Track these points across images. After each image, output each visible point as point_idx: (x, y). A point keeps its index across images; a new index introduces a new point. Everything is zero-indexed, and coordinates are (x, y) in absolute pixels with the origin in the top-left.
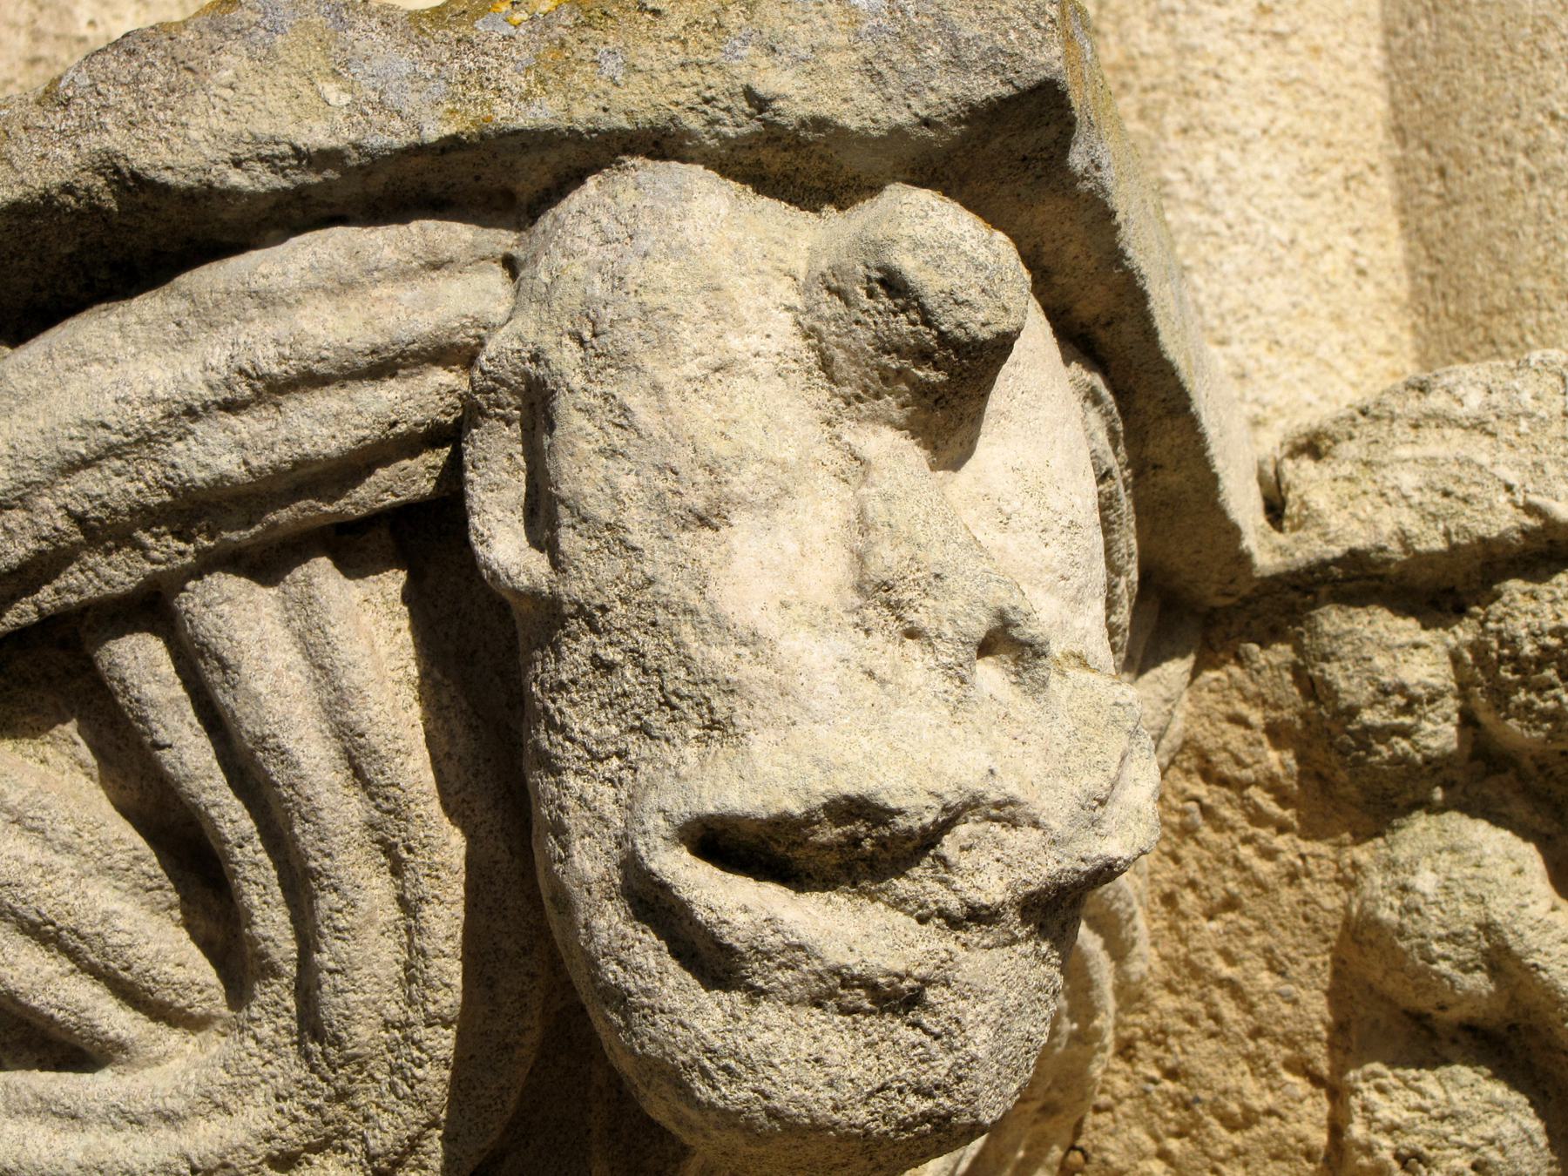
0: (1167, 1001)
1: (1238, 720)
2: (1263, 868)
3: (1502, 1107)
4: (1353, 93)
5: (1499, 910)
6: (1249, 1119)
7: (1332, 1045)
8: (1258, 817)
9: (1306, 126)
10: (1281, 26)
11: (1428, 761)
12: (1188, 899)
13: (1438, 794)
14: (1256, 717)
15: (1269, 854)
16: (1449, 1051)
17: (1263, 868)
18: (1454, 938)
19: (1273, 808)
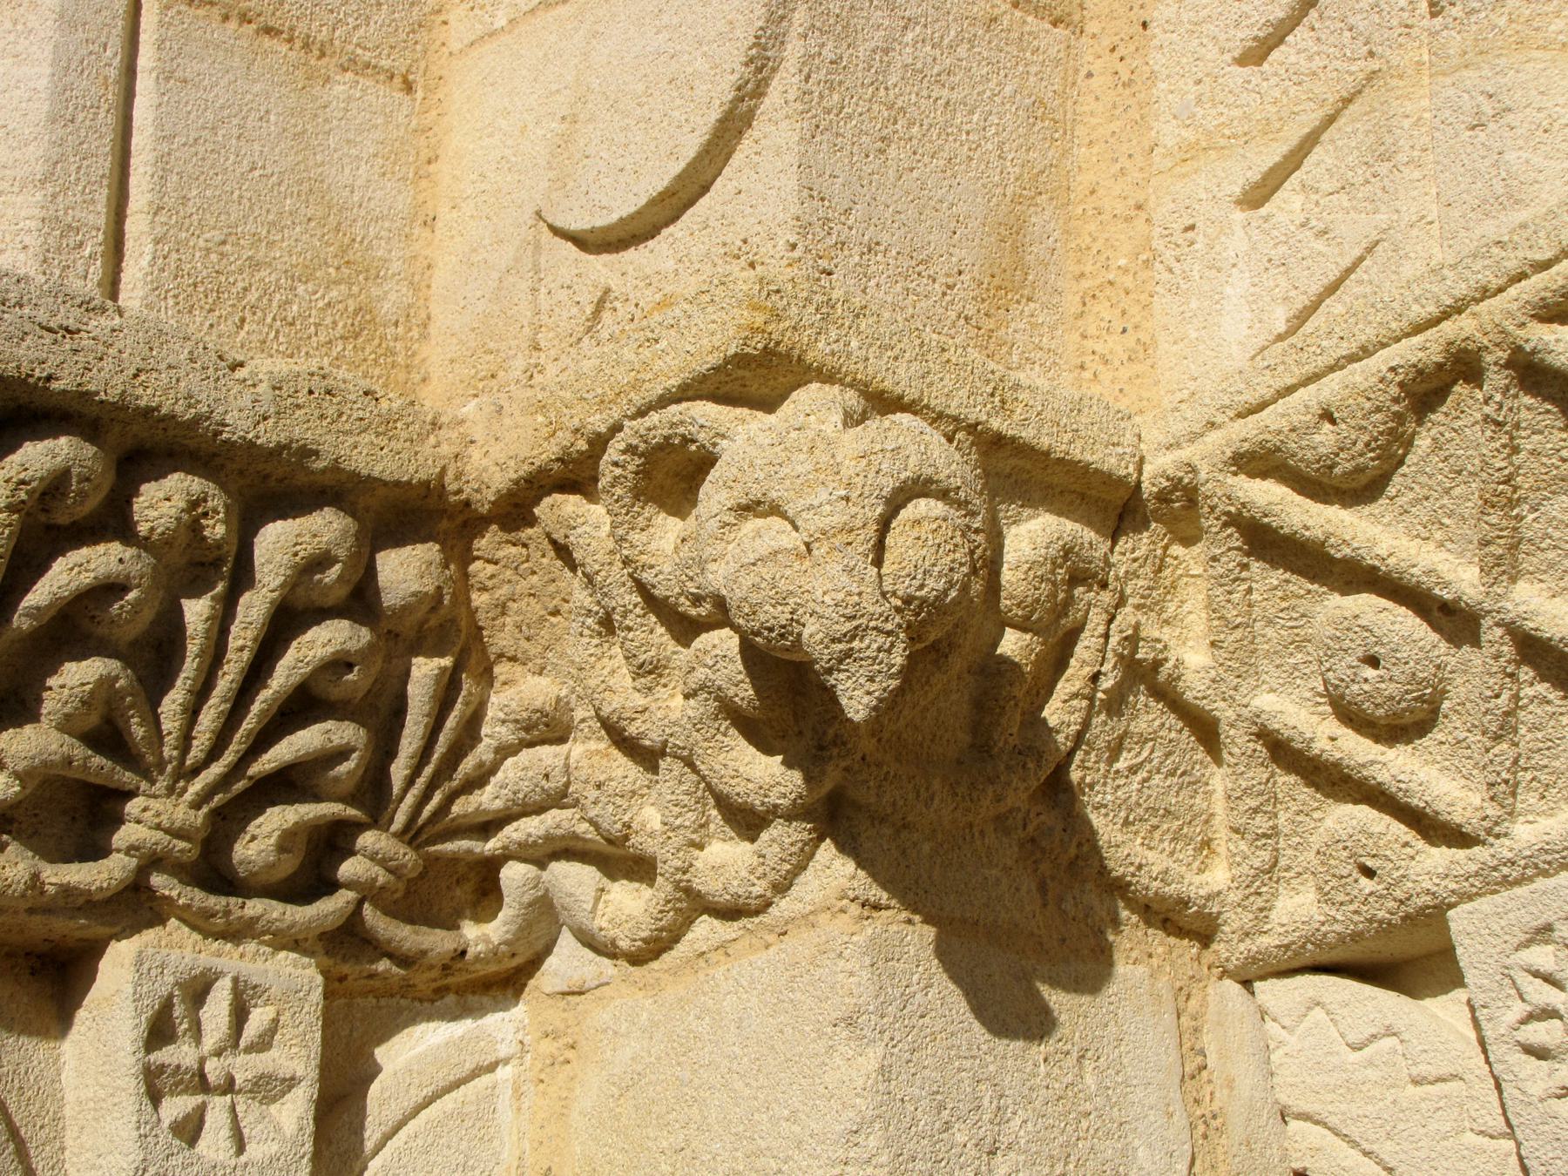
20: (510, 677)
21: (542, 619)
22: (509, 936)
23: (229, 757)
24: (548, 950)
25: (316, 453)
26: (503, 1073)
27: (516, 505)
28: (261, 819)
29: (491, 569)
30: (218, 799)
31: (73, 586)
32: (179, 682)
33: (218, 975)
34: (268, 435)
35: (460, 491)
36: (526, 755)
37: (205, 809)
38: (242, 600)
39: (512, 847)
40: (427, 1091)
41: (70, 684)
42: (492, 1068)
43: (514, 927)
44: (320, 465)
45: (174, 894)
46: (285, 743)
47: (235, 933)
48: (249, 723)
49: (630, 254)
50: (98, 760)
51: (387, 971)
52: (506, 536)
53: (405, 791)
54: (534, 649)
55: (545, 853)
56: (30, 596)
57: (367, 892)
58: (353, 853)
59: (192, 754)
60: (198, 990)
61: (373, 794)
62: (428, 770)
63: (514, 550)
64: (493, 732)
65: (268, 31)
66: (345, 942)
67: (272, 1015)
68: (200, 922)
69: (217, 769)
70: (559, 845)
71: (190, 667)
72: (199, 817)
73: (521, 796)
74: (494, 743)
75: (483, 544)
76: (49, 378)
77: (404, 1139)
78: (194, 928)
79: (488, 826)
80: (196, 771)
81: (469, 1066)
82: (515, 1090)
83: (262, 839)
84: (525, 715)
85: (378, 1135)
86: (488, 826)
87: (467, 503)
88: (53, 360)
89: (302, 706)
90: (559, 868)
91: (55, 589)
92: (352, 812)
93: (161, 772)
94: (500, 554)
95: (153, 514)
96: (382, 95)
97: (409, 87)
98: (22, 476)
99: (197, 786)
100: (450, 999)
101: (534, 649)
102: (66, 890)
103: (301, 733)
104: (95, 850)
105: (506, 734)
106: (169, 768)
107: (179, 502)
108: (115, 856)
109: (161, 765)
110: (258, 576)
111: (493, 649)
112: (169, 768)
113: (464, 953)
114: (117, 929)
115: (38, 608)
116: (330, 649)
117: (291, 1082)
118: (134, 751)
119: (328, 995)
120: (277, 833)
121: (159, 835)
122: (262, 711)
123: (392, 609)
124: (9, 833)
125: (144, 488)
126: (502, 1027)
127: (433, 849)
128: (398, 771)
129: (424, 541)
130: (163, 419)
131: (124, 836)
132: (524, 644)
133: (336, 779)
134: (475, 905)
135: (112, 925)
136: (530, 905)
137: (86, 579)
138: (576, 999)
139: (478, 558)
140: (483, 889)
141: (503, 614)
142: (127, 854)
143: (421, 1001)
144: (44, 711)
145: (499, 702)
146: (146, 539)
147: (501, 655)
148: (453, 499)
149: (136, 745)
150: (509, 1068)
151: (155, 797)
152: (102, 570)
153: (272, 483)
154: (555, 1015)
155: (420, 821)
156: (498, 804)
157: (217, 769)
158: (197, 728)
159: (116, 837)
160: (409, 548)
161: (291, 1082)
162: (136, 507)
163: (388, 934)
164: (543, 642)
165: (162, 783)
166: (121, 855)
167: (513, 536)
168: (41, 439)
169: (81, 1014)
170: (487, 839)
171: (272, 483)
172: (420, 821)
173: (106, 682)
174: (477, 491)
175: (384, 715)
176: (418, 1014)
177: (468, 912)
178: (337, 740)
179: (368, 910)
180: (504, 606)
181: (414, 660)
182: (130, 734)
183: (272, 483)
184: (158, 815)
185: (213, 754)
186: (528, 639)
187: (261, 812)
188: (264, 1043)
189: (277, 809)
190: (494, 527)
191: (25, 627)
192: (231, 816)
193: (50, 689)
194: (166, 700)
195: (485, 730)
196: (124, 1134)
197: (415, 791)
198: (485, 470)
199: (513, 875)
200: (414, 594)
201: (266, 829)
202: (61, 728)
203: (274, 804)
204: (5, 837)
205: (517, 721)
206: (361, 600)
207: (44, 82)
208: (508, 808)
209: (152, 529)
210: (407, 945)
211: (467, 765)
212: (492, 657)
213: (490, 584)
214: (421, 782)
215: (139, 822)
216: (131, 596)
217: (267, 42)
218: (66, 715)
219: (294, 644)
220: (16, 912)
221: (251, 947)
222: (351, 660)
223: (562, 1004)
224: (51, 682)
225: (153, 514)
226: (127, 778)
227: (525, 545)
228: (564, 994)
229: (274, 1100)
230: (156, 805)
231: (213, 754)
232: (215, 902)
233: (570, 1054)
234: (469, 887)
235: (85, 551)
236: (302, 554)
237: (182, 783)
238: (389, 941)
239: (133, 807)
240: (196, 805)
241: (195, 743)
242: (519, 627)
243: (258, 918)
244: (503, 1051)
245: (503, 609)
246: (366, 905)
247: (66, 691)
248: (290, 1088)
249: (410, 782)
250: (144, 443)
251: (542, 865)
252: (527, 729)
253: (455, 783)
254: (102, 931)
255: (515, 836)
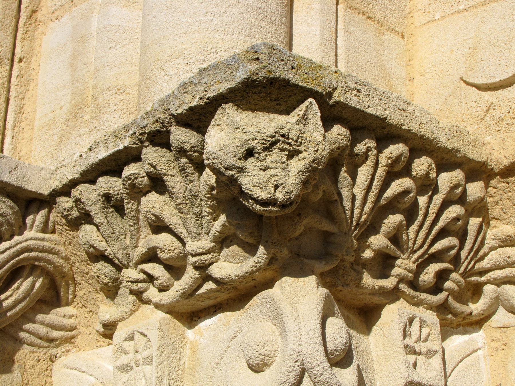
0: (72, 258)
1: (57, 216)
2: (71, 237)
3: (106, 267)
4: (133, 99)
5: (88, 239)
6: (87, 274)
7: (90, 260)
8: (67, 230)
9: (124, 107)
10: (121, 91)
11: (76, 218)
12: (66, 243)
13: (83, 222)
14: (59, 215)
15: (70, 235)
16: (100, 259)
17: (71, 237)
18: (85, 244)
19: (67, 228)
20: (496, 225)
21: (511, 207)
22: (485, 308)
23: (425, 247)
24: (493, 313)
25: (460, 151)
26: (480, 352)
27: (508, 170)
28: (428, 268)
29: (495, 190)
30: (420, 260)
31: (398, 191)
32: (416, 223)
33: (416, 317)
34: (450, 145)
35: (491, 165)
36: (499, 250)
37: (416, 264)
38: (434, 197)
39: (491, 280)
40: (461, 357)
41: (391, 222)
42: (476, 351)
43: (487, 306)
44: (460, 155)
45: (406, 290)
46: (438, 243)
47: (417, 304)
48: (431, 237)
49: (500, 91)
50: (393, 247)
51: (451, 318)
52: (502, 180)
53: (465, 260)
54: (506, 216)
55: (499, 283)
56: (386, 194)
57: (451, 292)
58: (448, 280)
59: (416, 246)
60: (411, 321)
61: (456, 261)
62: (472, 254)
63: (503, 184)
64: (489, 242)
65: (369, 18)
66: (442, 309)
67: (429, 331)
68: (410, 300)
69: (422, 251)
70: (508, 279)
71: (420, 218)
72: (414, 266)
73: (498, 263)
74: (490, 246)
75: (493, 182)
76: (402, 125)
77: (457, 372)
78: (407, 302)
79: (482, 273)
80: (415, 252)
81: (471, 350)
82: (485, 358)
83: (428, 275)
84: (504, 237)
85: (450, 371)
86: (482, 273)
87: (492, 169)
88: (402, 119)
89: (443, 233)
90: (504, 286)
91: (393, 192)
92: (451, 266)
93: (407, 252)
94: (499, 185)
95: (418, 169)
96: (397, 39)
97: (403, 37)
98: (390, 155)
99: (415, 256)
100: (461, 328)
101: (506, 216)
102: (381, 288)
103: (442, 241)
104: (385, 276)
105: (494, 243)
106: (409, 250)
107: (426, 165)
108: (391, 277)
109: (407, 250)
110: (440, 190)
111: (491, 216)
112: (409, 250)
113: (471, 313)
114: (389, 301)
115: (388, 198)
116: (456, 214)
117: (436, 352)
118: (401, 244)
119: (441, 325)
120: (434, 272)
121: (405, 271)
122: (435, 233)
123: (470, 202)
124: (365, 269)
125: (415, 160)
126: (478, 337)
127: (468, 279)
128: (464, 254)
129: (480, 181)
130: (425, 139)
131: (396, 271)
132: (503, 214)
133: (450, 255)
134: (472, 298)
135: (388, 300)
136: (494, 298)
137: (401, 189)
138: (506, 329)
139: (491, 187)
140: (476, 291)
141: (496, 205)
142: (396, 277)
143: (453, 328)
144: (382, 231)
145: (490, 233)
146: (414, 177)
147: (494, 218)
148: (489, 167)
149: (402, 242)
150: (481, 351)
151: (404, 259)
152: (406, 186)
153: (446, 160)
154: (497, 334)
155: (467, 270)
156: (489, 266)
157: (422, 251)
158: (418, 238)
159: (392, 272)
160: (476, 183)
161: (436, 352)
162: (412, 167)
163: (455, 306)
164: (510, 214)
165: (407, 254)
166: (394, 277)
167: (505, 180)
168: (395, 144)
169: (375, 328)
170: (481, 277)
171: (444, 161)
172: (467, 270)
173: (401, 222)
174: (496, 165)
175: (463, 236)
176: (453, 332)
177: (470, 300)
178: (452, 243)
179: (450, 298)
180: (497, 202)
181: (470, 219)
182: (402, 238)
183: (444, 161)
184: (406, 265)
185: (421, 246)
186: (504, 213)
187: (428, 265)
188: (426, 340)
189: (433, 264)
190: (498, 177)
191: (384, 203)
192: (421, 266)
193: (384, 223)
194: (411, 228)
195: (486, 242)
196: (401, 366)
197: (468, 260)
198: (500, 158)
199: (489, 289)
200: (478, 197)
201: (430, 271)
202: (385, 236)
203: (432, 263)
204: (364, 270)
205: (500, 239)
206: (462, 200)
207: (318, 32)
208: (492, 267)
209: (417, 174)
210: (459, 310)
211: (481, 253)
212: (490, 218)
213: (494, 195)
214: (470, 257)
215: (399, 267)
216: (411, 195)
217: (369, 21)
218: (388, 232)
219: (445, 212)
220: (366, 294)
221: (421, 308)
222: (460, 218)
223: (500, 331)
224: (385, 221)
225: (418, 169)
226: (398, 252)
227: (508, 183)
228: (500, 328)
229: (430, 358)
230: (405, 262)
231: (421, 246)
232: (416, 294)
233: (504, 347)
234: (471, 292)
235: (400, 180)
236: (453, 183)
237: (411, 255)
238: (454, 308)
239: (398, 262)
240: (414, 263)
241: (417, 242)
242: (502, 209)
243: (425, 299)
244: (480, 345)
245: (497, 203)
246: (450, 297)
247: (390, 224)
248: (435, 354)
249: (467, 257)
250: (420, 145)
251: (498, 285)
252: (503, 242)
253: (477, 258)
254: (385, 301)
255: (493, 276)
